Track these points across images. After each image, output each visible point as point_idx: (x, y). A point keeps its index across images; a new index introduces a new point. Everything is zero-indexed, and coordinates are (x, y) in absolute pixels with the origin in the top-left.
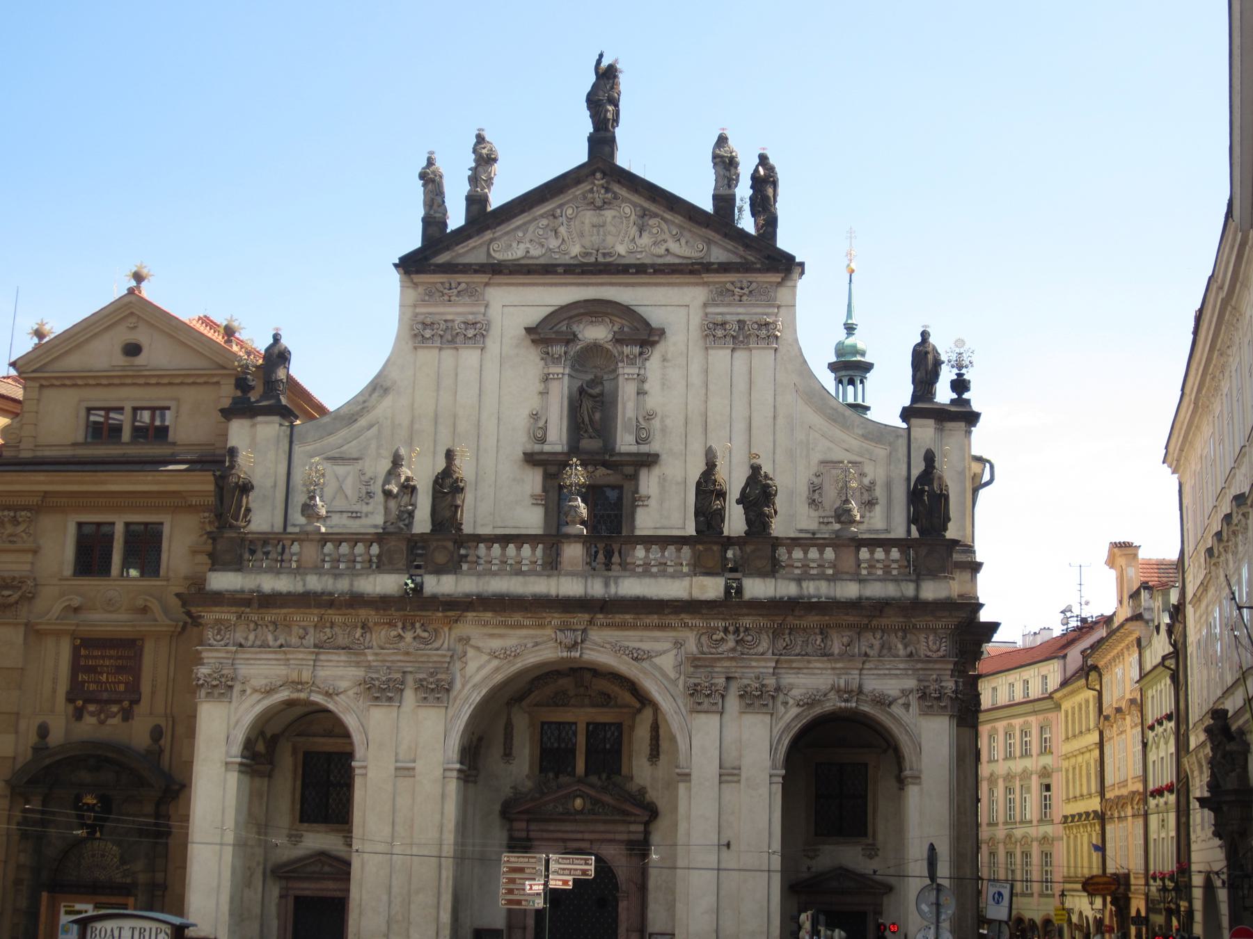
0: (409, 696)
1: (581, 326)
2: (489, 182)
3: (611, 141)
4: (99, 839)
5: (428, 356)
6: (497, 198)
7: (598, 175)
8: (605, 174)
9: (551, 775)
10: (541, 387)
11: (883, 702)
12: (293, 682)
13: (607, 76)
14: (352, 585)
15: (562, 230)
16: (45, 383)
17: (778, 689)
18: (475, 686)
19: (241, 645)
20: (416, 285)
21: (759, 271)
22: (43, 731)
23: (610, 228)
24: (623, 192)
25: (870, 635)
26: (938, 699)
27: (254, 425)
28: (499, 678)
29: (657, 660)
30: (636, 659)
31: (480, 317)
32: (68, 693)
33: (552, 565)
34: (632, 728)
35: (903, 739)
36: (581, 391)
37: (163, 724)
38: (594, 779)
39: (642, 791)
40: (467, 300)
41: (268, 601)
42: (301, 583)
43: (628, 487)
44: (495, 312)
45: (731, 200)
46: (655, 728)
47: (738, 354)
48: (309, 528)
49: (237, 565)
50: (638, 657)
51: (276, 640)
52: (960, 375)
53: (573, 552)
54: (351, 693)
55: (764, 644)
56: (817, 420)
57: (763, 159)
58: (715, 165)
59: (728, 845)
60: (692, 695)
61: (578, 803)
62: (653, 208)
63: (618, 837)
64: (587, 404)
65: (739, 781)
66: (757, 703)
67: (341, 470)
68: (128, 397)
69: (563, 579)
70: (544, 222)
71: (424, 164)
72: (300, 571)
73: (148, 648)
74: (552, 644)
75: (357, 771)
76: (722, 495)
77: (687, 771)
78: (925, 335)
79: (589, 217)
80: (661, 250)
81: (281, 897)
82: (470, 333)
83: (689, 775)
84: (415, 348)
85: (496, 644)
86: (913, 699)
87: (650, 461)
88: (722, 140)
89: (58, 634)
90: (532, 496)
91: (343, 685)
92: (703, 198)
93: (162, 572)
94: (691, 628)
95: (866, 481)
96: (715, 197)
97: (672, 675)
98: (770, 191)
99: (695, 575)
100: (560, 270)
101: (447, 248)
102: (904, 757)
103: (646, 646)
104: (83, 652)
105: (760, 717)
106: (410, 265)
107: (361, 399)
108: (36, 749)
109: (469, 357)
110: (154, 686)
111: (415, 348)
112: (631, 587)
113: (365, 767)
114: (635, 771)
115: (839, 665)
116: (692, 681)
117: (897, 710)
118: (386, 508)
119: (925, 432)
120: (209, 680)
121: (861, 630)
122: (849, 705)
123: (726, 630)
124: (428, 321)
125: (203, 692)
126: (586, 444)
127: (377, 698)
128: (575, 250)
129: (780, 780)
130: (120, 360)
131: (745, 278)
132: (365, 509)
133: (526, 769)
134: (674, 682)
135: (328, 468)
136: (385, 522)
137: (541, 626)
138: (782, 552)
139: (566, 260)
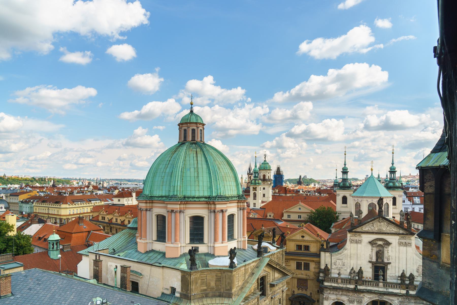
5: (352, 245)
10: (371, 250)
27: (325, 253)
29: (395, 301)
33: (377, 285)
43: (386, 267)
44: (362, 238)
48: (339, 277)
50: (392, 300)
53: (381, 284)
55: (413, 301)
67: (339, 261)
68: (303, 244)
85: (369, 296)
89: (295, 278)
93: (310, 270)
99: (401, 289)
103: (393, 299)
110: (310, 286)
112: (390, 290)
123: (406, 299)
126: (379, 260)
132: (343, 267)
135: (337, 260)
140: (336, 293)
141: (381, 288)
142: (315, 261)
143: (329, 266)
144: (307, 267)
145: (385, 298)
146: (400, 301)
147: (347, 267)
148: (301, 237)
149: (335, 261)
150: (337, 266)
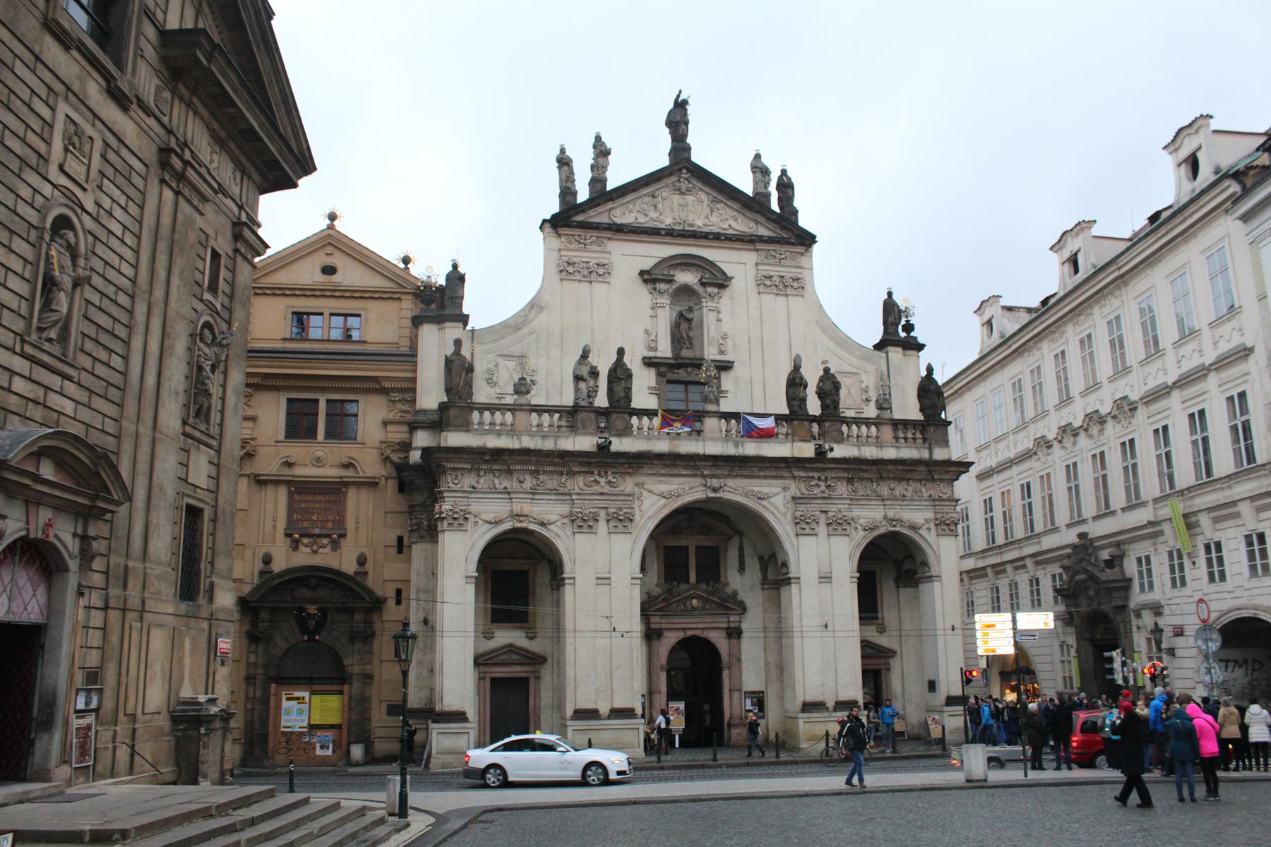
0: (602, 526)
1: (676, 273)
2: (605, 168)
3: (688, 149)
4: (317, 641)
6: (614, 180)
7: (684, 171)
8: (689, 170)
9: (675, 583)
10: (651, 312)
11: (914, 528)
12: (517, 515)
13: (680, 106)
14: (556, 443)
15: (660, 206)
16: (258, 291)
17: (852, 519)
18: (650, 517)
19: (474, 487)
20: (560, 235)
21: (792, 244)
22: (267, 560)
23: (690, 207)
24: (699, 185)
25: (904, 483)
26: (948, 525)
28: (666, 512)
30: (760, 498)
31: (606, 261)
32: (285, 529)
34: (726, 550)
35: (928, 551)
36: (681, 315)
37: (366, 551)
38: (704, 586)
39: (735, 593)
40: (597, 248)
41: (498, 454)
42: (517, 442)
45: (768, 196)
46: (741, 549)
47: (779, 297)
49: (466, 426)
51: (500, 484)
52: (908, 321)
54: (559, 523)
55: (842, 489)
56: (831, 345)
57: (784, 172)
58: (753, 172)
59: (826, 626)
60: (798, 523)
61: (695, 602)
62: (719, 197)
63: (722, 625)
64: (684, 326)
65: (831, 582)
66: (840, 528)
69: (707, 443)
70: (647, 199)
71: (558, 152)
72: (512, 431)
73: (352, 494)
74: (702, 488)
75: (567, 581)
76: (805, 387)
77: (797, 575)
78: (890, 294)
79: (677, 198)
80: (726, 226)
81: (480, 679)
82: (601, 271)
83: (799, 578)
84: (561, 280)
86: (932, 525)
87: (725, 367)
88: (758, 157)
90: (649, 388)
91: (553, 518)
92: (751, 195)
94: (794, 477)
95: (863, 386)
96: (756, 194)
97: (782, 509)
98: (790, 190)
99: (794, 441)
100: (663, 232)
101: (583, 211)
102: (925, 564)
103: (765, 490)
104: (296, 497)
105: (842, 537)
106: (556, 223)
107: (523, 314)
108: (262, 573)
109: (600, 289)
111: (561, 280)
112: (751, 448)
113: (574, 578)
114: (730, 580)
115: (889, 503)
116: (798, 514)
117: (921, 532)
118: (577, 390)
119: (895, 353)
120: (451, 513)
121: (901, 480)
122: (896, 529)
123: (819, 479)
124: (572, 261)
125: (445, 523)
127: (580, 527)
128: (668, 221)
129: (856, 580)
130: (319, 278)
131: (782, 249)
133: (655, 580)
134: (784, 515)
135: (500, 360)
136: (576, 399)
137: (695, 476)
138: (844, 428)
139: (663, 226)
140: (506, 483)
141: (714, 439)
142: (386, 385)
143: (465, 352)
144: (340, 427)
145: (736, 490)
146: (793, 498)
147: (547, 393)
148: (318, 270)
149: (491, 366)
150: (498, 391)
